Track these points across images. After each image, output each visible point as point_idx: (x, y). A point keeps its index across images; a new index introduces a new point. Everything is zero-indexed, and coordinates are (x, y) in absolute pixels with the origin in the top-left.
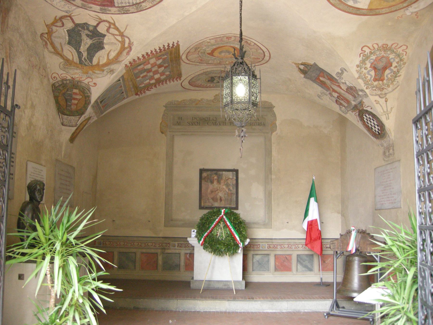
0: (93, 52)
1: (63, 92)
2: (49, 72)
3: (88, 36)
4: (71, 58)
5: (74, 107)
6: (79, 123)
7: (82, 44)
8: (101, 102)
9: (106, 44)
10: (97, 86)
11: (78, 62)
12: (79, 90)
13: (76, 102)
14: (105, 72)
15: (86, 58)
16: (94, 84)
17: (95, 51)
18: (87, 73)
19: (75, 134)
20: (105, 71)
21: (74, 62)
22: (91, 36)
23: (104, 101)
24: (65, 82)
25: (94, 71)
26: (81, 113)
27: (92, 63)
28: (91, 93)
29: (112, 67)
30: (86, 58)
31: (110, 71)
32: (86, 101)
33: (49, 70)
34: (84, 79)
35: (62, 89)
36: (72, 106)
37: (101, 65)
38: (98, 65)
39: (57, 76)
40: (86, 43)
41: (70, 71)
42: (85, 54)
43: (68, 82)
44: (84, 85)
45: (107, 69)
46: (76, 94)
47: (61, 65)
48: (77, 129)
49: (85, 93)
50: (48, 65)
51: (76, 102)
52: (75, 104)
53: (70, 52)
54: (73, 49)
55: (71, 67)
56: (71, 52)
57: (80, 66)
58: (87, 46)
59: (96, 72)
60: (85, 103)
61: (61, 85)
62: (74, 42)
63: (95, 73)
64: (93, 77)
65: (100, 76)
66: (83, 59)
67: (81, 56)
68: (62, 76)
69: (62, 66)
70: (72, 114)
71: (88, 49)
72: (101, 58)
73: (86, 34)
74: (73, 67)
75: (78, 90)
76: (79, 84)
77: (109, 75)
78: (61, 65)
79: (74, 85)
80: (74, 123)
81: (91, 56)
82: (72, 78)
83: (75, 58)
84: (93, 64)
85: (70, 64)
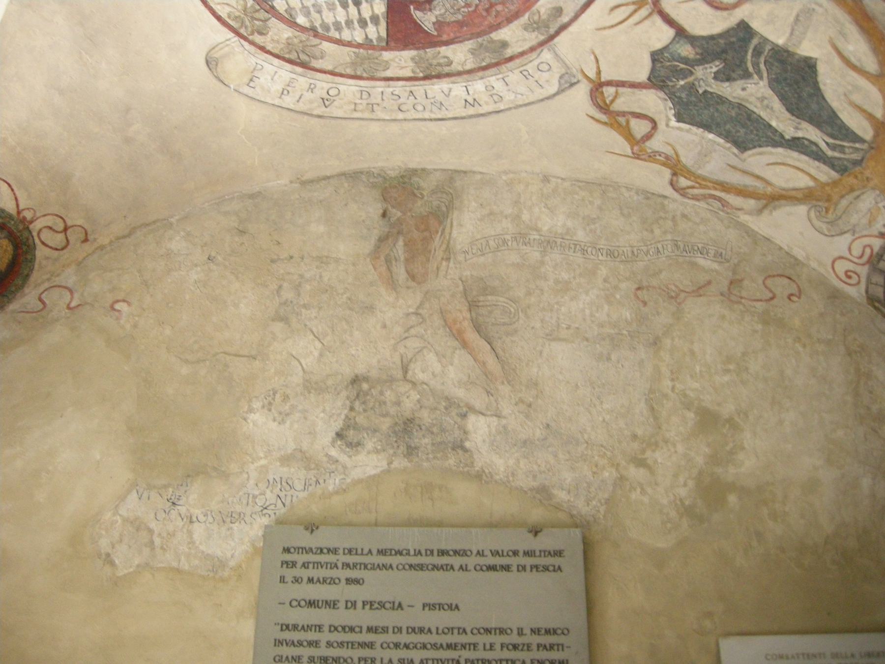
0: (814, 106)
2: (822, 271)
4: (804, 182)
11: (834, 175)
15: (830, 141)
17: (811, 96)
21: (828, 184)
27: (862, 141)
33: (814, 264)
39: (851, 266)
40: (762, 99)
50: (799, 254)
54: (770, 149)
56: (784, 164)
58: (777, 104)
66: (830, 153)
69: (824, 227)
71: (787, 110)
72: (857, 98)
74: (844, 203)
83: (813, 172)
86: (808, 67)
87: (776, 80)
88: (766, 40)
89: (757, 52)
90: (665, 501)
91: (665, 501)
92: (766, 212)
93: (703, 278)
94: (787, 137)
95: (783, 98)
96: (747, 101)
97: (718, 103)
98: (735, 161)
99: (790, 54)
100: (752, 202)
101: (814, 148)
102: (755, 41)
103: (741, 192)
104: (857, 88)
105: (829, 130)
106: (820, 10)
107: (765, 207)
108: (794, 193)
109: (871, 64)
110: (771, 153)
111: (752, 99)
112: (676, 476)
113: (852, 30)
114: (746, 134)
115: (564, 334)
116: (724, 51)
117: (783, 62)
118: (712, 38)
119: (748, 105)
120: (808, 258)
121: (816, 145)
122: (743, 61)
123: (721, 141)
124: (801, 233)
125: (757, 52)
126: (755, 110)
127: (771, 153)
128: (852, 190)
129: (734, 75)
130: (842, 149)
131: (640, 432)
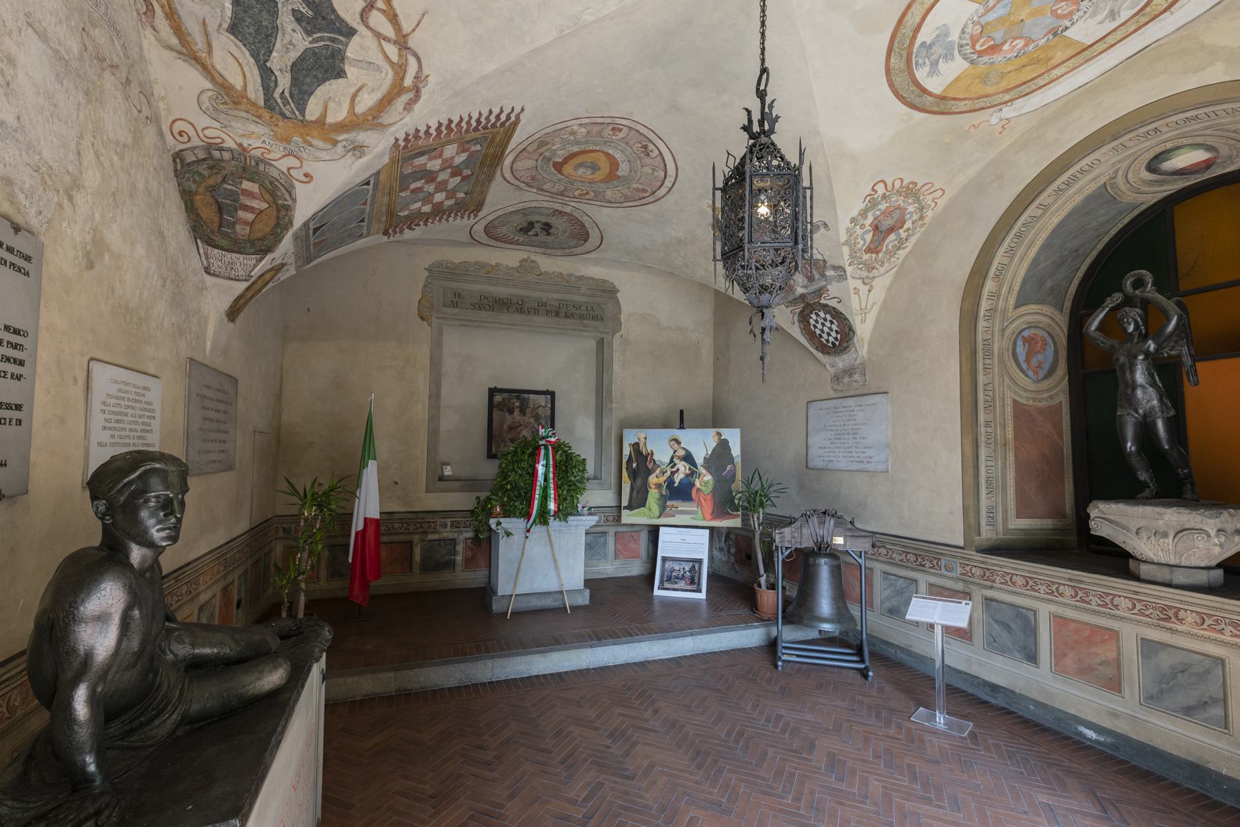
0: (308, 80)
1: (211, 181)
2: (163, 114)
3: (298, 17)
5: (242, 231)
6: (256, 272)
7: (278, 45)
8: (315, 230)
9: (358, 63)
10: (312, 184)
11: (261, 102)
12: (261, 185)
13: (250, 217)
14: (339, 148)
15: (287, 94)
16: (306, 175)
17: (315, 76)
18: (289, 142)
19: (242, 301)
20: (340, 145)
22: (309, 20)
23: (325, 232)
24: (216, 154)
25: (309, 138)
26: (263, 247)
28: (294, 201)
29: (363, 137)
30: (287, 94)
31: (354, 149)
32: (278, 218)
33: (162, 105)
34: (279, 156)
35: (206, 173)
36: (238, 227)
37: (331, 125)
38: (321, 122)
39: (192, 133)
40: (291, 43)
41: (234, 124)
42: (284, 82)
43: (227, 155)
44: (275, 174)
45: (346, 140)
46: (250, 194)
47: (205, 97)
48: (248, 288)
49: (279, 197)
50: (158, 91)
51: (250, 217)
52: (246, 223)
53: (233, 61)
55: (236, 113)
57: (267, 115)
58: (294, 55)
59: (315, 142)
60: (277, 224)
61: (205, 160)
62: (251, 30)
63: (311, 145)
64: (304, 155)
65: (324, 155)
66: (277, 95)
67: (272, 85)
68: (207, 132)
69: (206, 104)
70: (236, 246)
72: (331, 105)
73: (293, 10)
74: (245, 115)
75: (256, 186)
76: (261, 167)
77: (349, 158)
78: (205, 97)
79: (244, 169)
80: (241, 273)
81: (301, 94)
82: (241, 145)
83: (250, 88)
84: (308, 117)
85: (235, 103)
86: (341, 74)
87: (315, 54)
88: (347, 45)
89: (333, 40)
90: (78, 240)
91: (78, 240)
92: (175, 54)
93: (116, 59)
94: (268, 64)
95: (302, 58)
96: (284, 34)
97: (269, 12)
98: (212, 26)
99: (343, 60)
100: (174, 41)
101: (272, 85)
102: (341, 38)
103: (179, 30)
104: (339, 104)
105: (296, 92)
106: (383, 75)
107: (180, 53)
108: (217, 76)
109: (360, 108)
110: (244, 54)
111: (288, 38)
112: (85, 222)
113: (378, 95)
114: (250, 34)
115: (36, 25)
116: (324, 18)
117: (333, 56)
118: (334, 11)
119: (280, 33)
120: (163, 98)
121: (276, 85)
122: (320, 30)
123: (229, 14)
124: (181, 88)
125: (333, 40)
126: (279, 40)
127: (244, 54)
128: (259, 117)
129: (304, 24)
130: (286, 103)
131: (70, 169)
